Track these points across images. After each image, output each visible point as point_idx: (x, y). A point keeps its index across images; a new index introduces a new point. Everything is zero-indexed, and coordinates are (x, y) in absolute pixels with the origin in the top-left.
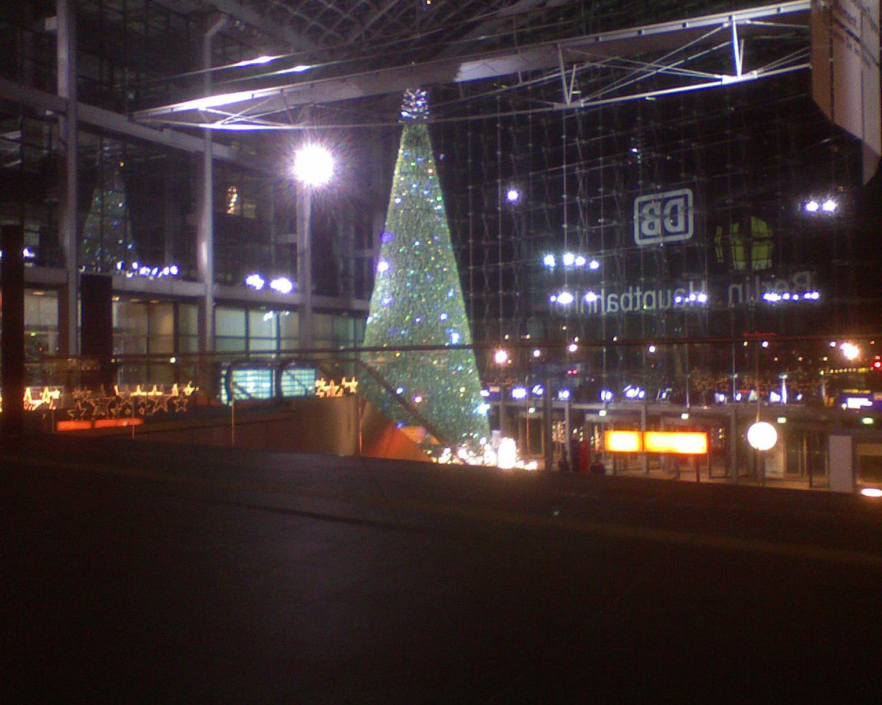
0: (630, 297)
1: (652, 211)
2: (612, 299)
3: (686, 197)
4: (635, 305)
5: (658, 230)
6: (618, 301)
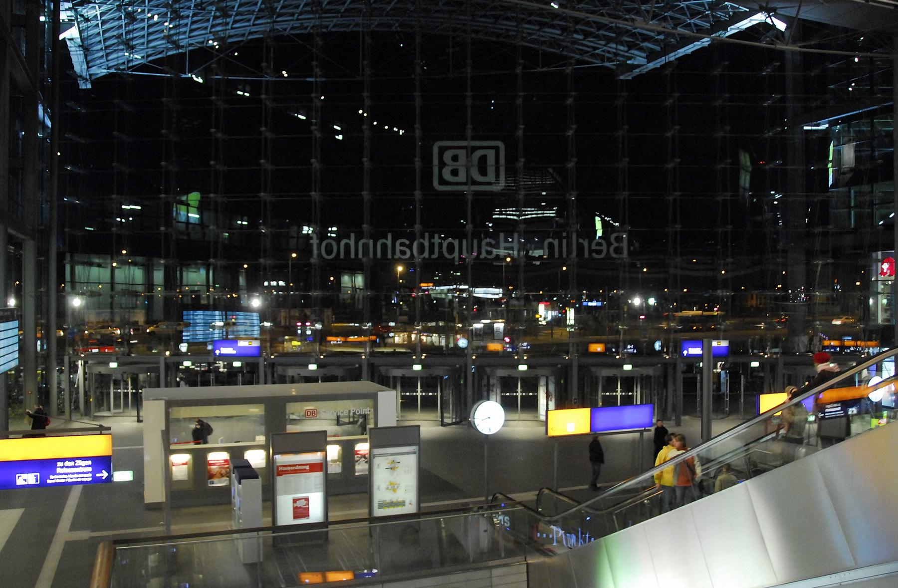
0: (426, 244)
1: (455, 158)
2: (402, 244)
3: (497, 149)
4: (432, 251)
5: (462, 177)
6: (410, 247)
